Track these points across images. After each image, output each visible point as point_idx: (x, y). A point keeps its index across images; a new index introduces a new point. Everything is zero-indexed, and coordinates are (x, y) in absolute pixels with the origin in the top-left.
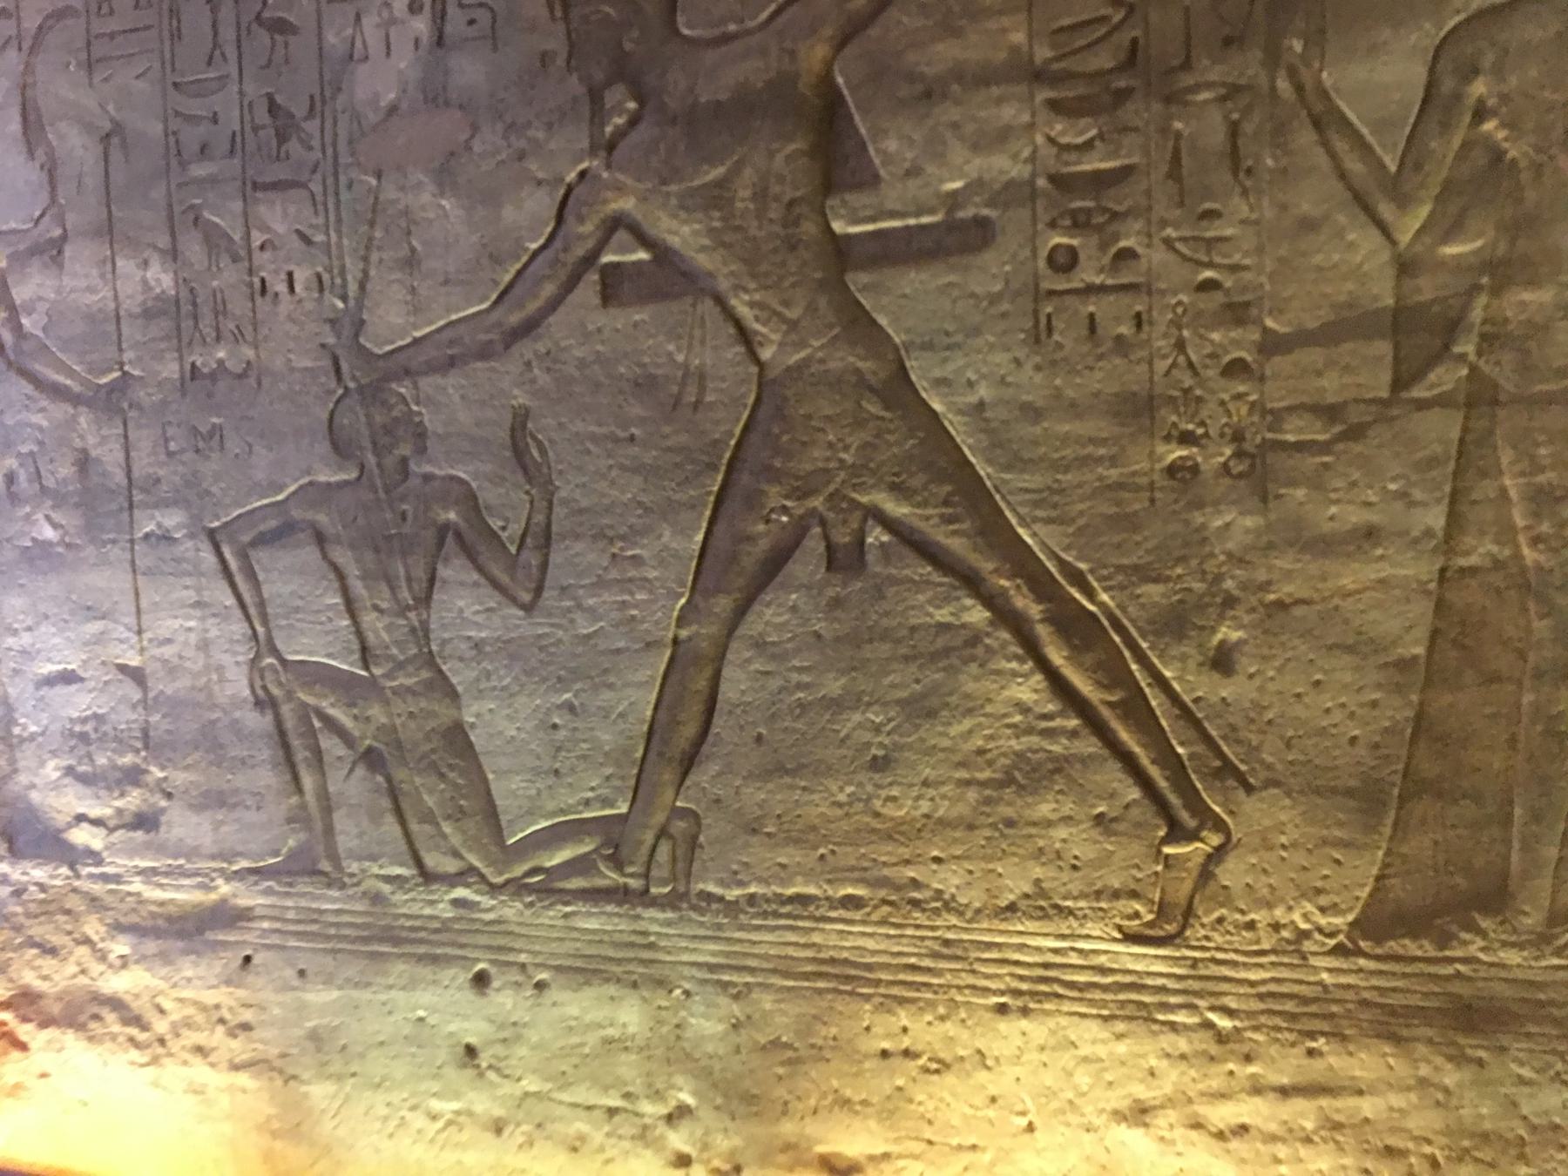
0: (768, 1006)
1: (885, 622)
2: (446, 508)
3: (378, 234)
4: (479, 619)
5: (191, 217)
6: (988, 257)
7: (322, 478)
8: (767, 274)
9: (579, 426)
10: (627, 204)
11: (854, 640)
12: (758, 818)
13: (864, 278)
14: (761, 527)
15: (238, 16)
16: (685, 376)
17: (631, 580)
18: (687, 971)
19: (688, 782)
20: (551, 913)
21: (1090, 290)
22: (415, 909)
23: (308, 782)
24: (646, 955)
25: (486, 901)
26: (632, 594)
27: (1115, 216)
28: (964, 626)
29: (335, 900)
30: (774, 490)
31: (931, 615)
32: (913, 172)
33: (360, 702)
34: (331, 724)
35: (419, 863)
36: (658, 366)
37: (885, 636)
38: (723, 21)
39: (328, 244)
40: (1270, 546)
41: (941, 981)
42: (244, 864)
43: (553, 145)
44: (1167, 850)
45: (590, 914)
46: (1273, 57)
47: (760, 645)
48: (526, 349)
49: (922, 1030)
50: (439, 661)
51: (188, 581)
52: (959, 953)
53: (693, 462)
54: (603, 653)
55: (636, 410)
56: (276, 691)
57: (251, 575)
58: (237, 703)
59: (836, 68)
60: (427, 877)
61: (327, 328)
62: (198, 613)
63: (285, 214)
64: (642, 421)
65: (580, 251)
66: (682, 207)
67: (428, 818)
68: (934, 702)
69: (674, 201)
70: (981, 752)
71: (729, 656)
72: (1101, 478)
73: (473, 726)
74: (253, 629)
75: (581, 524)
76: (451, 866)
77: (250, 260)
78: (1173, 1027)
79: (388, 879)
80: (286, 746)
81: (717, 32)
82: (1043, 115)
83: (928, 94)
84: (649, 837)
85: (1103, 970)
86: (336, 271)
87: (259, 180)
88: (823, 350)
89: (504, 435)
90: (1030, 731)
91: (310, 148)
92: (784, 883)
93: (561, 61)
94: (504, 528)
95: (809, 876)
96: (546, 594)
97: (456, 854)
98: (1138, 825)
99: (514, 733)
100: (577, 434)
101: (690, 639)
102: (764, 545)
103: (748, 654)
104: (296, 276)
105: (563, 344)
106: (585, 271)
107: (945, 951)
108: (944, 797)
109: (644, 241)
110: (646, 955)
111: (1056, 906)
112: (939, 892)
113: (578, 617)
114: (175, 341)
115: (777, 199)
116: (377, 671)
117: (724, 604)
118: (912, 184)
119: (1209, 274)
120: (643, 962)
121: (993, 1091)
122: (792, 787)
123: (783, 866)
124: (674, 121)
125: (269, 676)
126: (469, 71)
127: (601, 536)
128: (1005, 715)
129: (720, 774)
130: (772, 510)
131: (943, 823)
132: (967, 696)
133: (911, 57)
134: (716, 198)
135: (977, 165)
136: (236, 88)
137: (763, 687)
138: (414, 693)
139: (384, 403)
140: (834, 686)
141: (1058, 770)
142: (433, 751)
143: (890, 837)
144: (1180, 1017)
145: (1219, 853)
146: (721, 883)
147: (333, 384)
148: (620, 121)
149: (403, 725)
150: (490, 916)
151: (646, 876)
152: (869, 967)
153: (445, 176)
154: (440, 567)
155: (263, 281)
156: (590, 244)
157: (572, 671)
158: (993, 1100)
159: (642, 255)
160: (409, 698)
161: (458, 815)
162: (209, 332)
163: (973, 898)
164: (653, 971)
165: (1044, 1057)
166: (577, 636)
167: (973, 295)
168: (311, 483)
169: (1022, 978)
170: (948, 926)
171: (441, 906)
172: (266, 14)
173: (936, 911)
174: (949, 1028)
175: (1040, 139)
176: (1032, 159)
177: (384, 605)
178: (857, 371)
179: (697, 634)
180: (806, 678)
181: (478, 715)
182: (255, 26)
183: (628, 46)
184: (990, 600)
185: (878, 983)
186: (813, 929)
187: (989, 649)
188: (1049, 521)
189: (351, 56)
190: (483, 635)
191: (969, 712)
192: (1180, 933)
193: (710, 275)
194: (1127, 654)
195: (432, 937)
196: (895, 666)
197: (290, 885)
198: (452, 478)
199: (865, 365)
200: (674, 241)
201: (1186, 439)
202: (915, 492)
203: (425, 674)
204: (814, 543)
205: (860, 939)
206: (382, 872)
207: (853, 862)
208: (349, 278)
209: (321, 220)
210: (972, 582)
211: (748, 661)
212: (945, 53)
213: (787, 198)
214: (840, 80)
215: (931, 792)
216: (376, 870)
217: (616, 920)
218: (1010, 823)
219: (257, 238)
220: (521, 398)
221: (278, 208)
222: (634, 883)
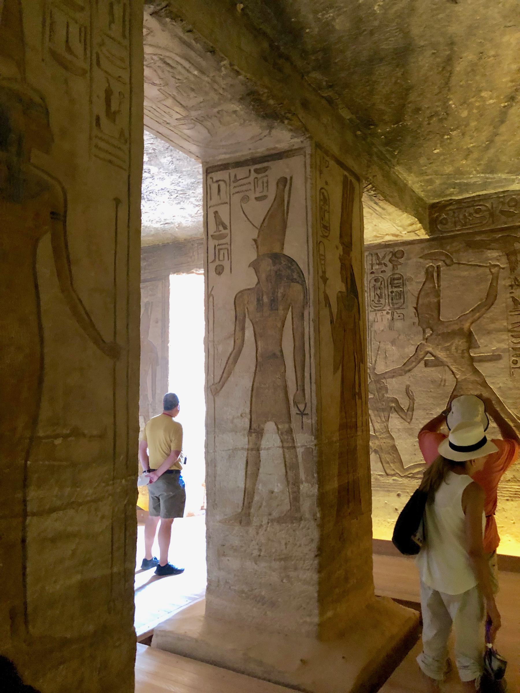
3: (379, 352)
6: (501, 361)
10: (430, 349)
13: (477, 364)
22: (385, 481)
25: (400, 479)
35: (386, 472)
48: (409, 374)
55: (432, 386)
60: (387, 475)
65: (421, 357)
67: (388, 463)
76: (393, 472)
79: (379, 475)
83: (488, 333)
89: (405, 390)
93: (417, 323)
97: (394, 470)
109: (433, 356)
121: (506, 516)
124: (439, 335)
126: (398, 324)
134: (448, 349)
135: (499, 345)
148: (429, 334)
150: (401, 482)
153: (393, 343)
156: (422, 356)
158: (506, 517)
159: (433, 358)
161: (394, 462)
165: (517, 509)
169: (511, 494)
175: (510, 341)
176: (508, 345)
183: (430, 322)
199: (478, 379)
200: (439, 356)
203: (388, 435)
212: (492, 326)
220: (408, 383)
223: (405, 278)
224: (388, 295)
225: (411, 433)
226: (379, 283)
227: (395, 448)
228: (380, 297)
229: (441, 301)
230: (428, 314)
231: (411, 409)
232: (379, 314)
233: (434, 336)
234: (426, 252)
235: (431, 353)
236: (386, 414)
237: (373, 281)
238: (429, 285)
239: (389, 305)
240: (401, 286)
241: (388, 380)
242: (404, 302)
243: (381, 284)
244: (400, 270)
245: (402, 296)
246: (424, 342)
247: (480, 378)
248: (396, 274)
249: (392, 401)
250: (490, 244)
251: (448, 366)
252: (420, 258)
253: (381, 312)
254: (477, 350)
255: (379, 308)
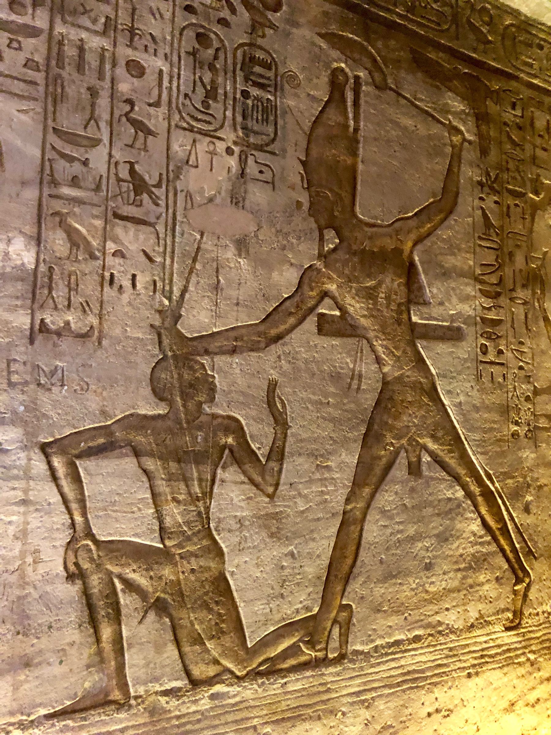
0: (382, 707)
1: (430, 498)
2: (226, 436)
4: (243, 504)
5: (57, 219)
7: (143, 412)
8: (389, 334)
9: (304, 395)
11: (418, 507)
12: (379, 604)
14: (383, 452)
15: (112, 108)
16: (353, 375)
17: (326, 479)
18: (345, 700)
19: (349, 589)
20: (275, 686)
21: (492, 363)
23: (106, 632)
24: (325, 697)
26: (326, 487)
27: (498, 337)
28: (456, 499)
29: (121, 721)
30: (388, 435)
31: (445, 494)
32: (441, 304)
33: (155, 567)
34: (130, 586)
36: (342, 368)
37: (430, 504)
38: (376, 218)
39: (164, 263)
40: (538, 465)
41: (450, 669)
42: (43, 712)
43: (300, 248)
44: (516, 588)
45: (297, 680)
46: (534, 293)
47: (383, 512)
49: (442, 696)
50: (214, 533)
51: (16, 484)
52: (455, 653)
53: (356, 418)
54: (310, 521)
55: (332, 389)
56: (86, 565)
57: (77, 479)
58: (48, 579)
59: (415, 253)
61: (157, 316)
62: (22, 509)
63: (136, 238)
64: (334, 395)
66: (357, 295)
67: (198, 640)
68: (448, 534)
69: (354, 291)
70: (461, 556)
71: (368, 517)
72: (495, 437)
73: (232, 573)
74: (72, 519)
75: (301, 448)
76: (212, 671)
77: (104, 260)
78: (519, 664)
79: (166, 693)
80: (90, 607)
81: (372, 221)
82: (478, 294)
83: (444, 274)
84: (329, 624)
85: (499, 646)
86: (167, 281)
87: (120, 212)
88: (409, 373)
90: (476, 544)
91: (157, 205)
92: (390, 635)
94: (259, 449)
95: (400, 628)
96: (281, 488)
97: (216, 662)
98: (507, 579)
99: (259, 575)
100: (302, 399)
101: (351, 510)
102: (384, 460)
103: (378, 517)
104: (138, 278)
105: (297, 349)
106: (309, 315)
107: (451, 653)
108: (450, 578)
110: (325, 697)
111: (485, 621)
112: (448, 625)
113: (298, 500)
114: (29, 302)
115: (394, 301)
116: (168, 543)
117: (367, 491)
118: (442, 308)
119: (521, 364)
120: (323, 702)
122: (395, 584)
123: (390, 627)
124: (355, 254)
125: (82, 554)
126: (258, 195)
127: (313, 455)
128: (469, 538)
129: (365, 582)
130: (387, 444)
131: (451, 591)
132: (458, 530)
133: (440, 258)
134: (370, 295)
136: (107, 151)
137: (384, 534)
138: (196, 556)
139: (191, 368)
140: (411, 530)
141: (485, 560)
142: (206, 593)
143: (432, 602)
144: (522, 659)
145: (529, 585)
146: (363, 643)
147: (156, 351)
148: (331, 246)
149: (186, 579)
150: (238, 699)
151: (326, 649)
152: (422, 671)
154: (219, 471)
155: (112, 275)
157: (294, 533)
159: (337, 313)
160: (193, 559)
161: (218, 634)
162: (62, 302)
163: (459, 625)
164: (329, 706)
166: (297, 512)
167: (459, 358)
168: (132, 415)
169: (475, 658)
170: (452, 641)
171: (203, 702)
172: (132, 115)
173: (447, 635)
174: (453, 692)
177: (181, 497)
178: (420, 382)
179: (355, 507)
180: (401, 527)
181: (237, 566)
182: (124, 119)
184: (464, 487)
185: (426, 678)
186: (401, 658)
187: (464, 509)
188: (482, 453)
189: (187, 162)
190: (244, 514)
191: (458, 538)
192: (520, 623)
193: (365, 329)
194: (503, 508)
195: (197, 726)
196: (435, 518)
197: (85, 719)
198: (229, 417)
200: (351, 310)
201: (517, 423)
202: (440, 439)
203: (205, 542)
204: (402, 460)
205: (419, 658)
206: (163, 688)
207: (418, 618)
208: (175, 289)
209: (161, 249)
210: (457, 479)
211: (377, 520)
212: (450, 261)
213: (398, 302)
214: (417, 258)
215: (446, 577)
216: (158, 688)
217: (311, 680)
218: (471, 587)
219: (111, 247)
220: (274, 375)
221: (131, 233)
222: (320, 654)
223: (281, 70)
224: (235, 99)
225: (274, 529)
226: (211, 52)
227: (222, 586)
228: (211, 94)
229: (360, 167)
230: (331, 190)
231: (278, 453)
232: (203, 145)
233: (341, 255)
234: (333, 28)
235: (333, 298)
236: (207, 469)
237: (190, 34)
238: (333, 116)
239: (235, 130)
240: (272, 89)
241: (217, 359)
242: (276, 133)
243: (216, 58)
244: (269, 40)
245: (272, 118)
246: (319, 264)
247: (426, 378)
248: (261, 48)
249: (227, 431)
250: (450, 80)
251: (367, 340)
252: (319, 35)
253: (208, 139)
254: (425, 310)
255: (205, 127)
